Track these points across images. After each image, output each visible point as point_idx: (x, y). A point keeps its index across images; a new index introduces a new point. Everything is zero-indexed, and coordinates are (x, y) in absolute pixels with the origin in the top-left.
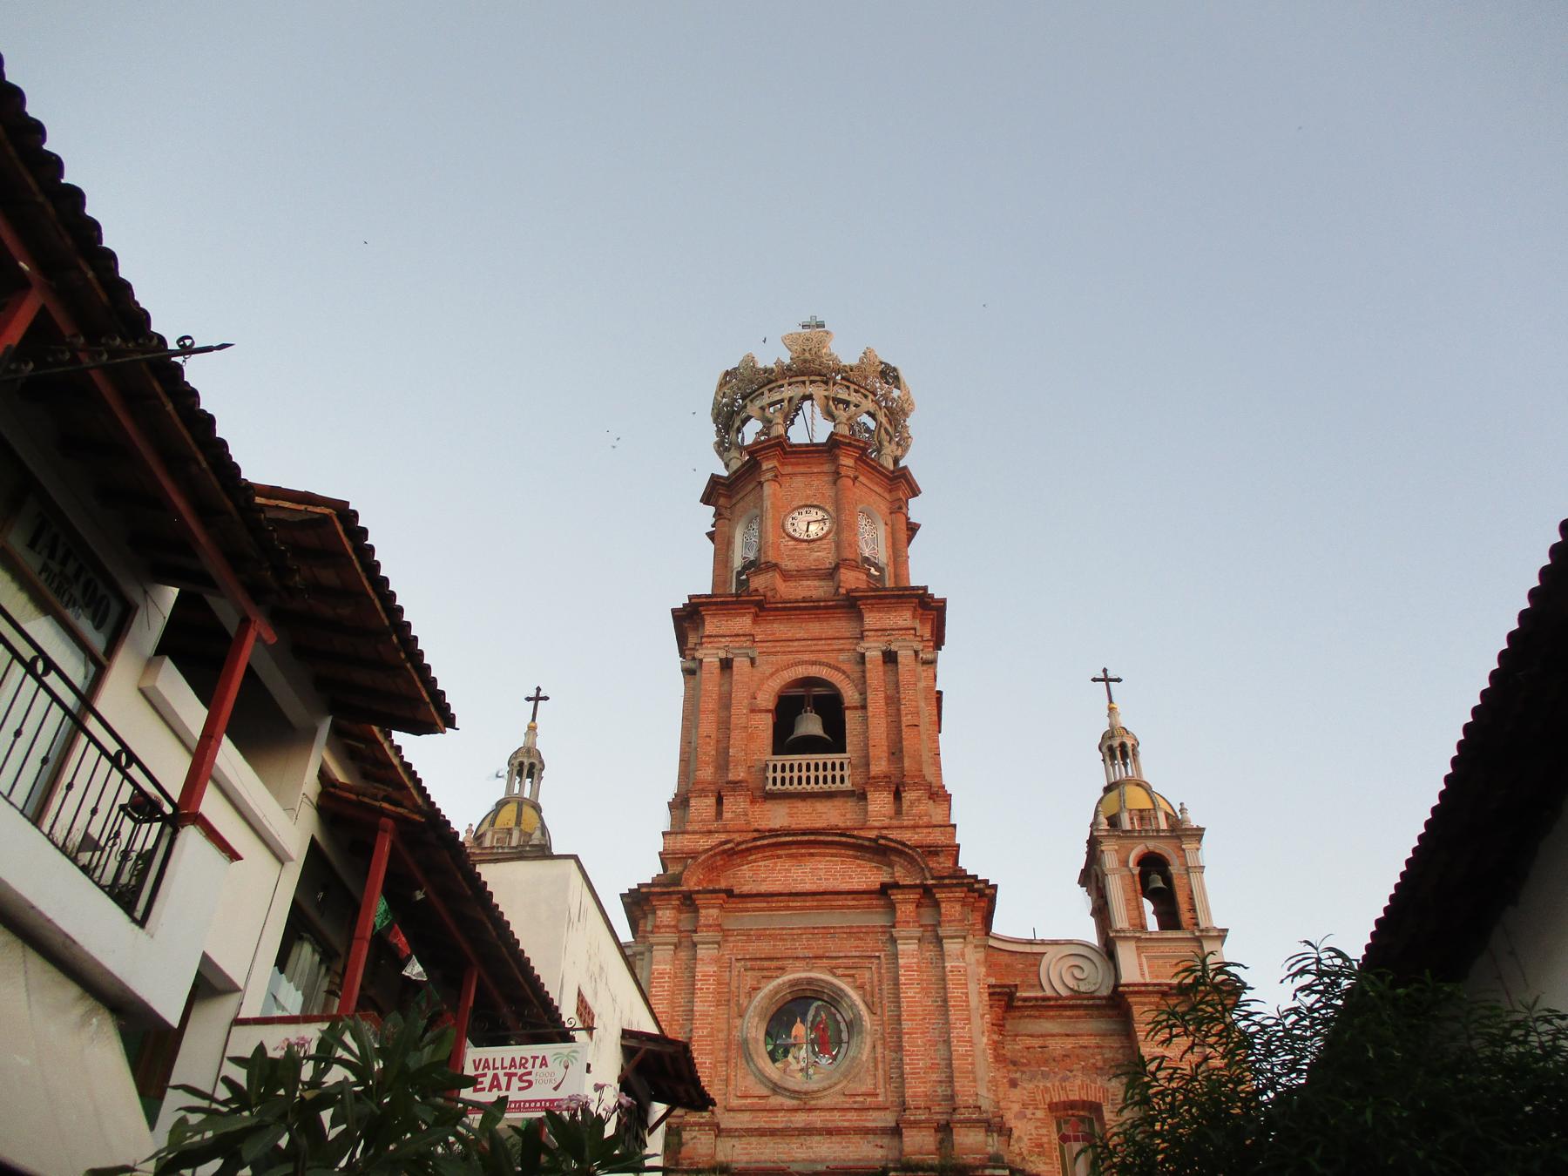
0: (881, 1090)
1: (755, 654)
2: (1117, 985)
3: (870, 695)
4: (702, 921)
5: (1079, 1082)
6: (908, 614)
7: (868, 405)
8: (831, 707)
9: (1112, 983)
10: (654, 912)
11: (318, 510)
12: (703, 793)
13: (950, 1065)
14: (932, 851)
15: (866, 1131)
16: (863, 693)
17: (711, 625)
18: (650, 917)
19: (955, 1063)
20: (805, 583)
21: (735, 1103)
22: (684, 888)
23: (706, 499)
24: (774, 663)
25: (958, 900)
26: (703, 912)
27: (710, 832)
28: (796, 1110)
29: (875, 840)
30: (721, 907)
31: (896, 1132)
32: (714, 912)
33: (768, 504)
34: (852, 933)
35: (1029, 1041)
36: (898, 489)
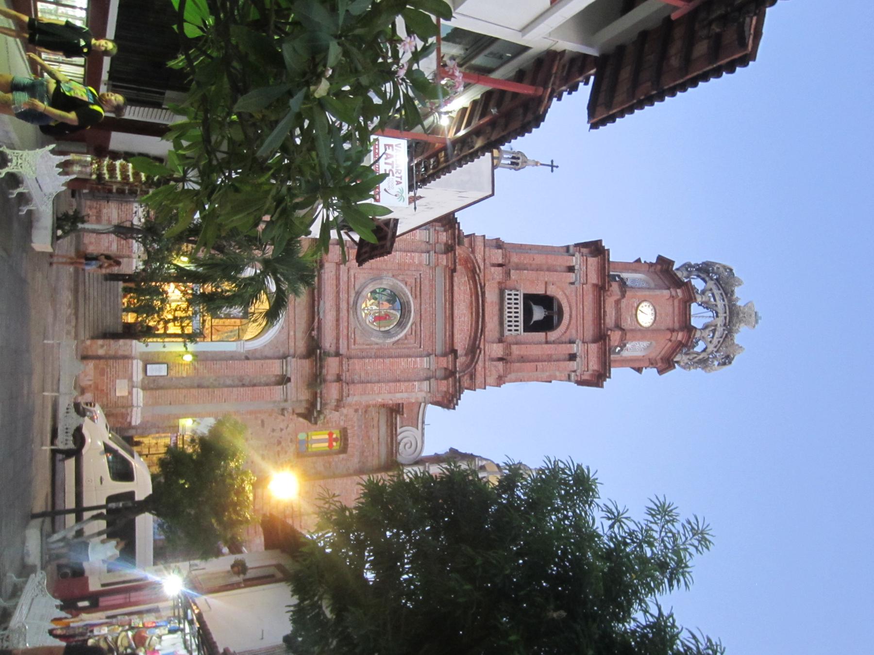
0: (357, 347)
1: (577, 284)
2: (402, 465)
3: (552, 346)
4: (440, 256)
5: (357, 443)
6: (596, 367)
7: (711, 348)
8: (546, 325)
9: (403, 462)
10: (446, 231)
11: (751, 42)
12: (504, 256)
13: (368, 382)
14: (472, 377)
15: (338, 339)
16: (554, 342)
17: (593, 261)
18: (442, 229)
19: (369, 385)
22: (457, 247)
23: (660, 259)
24: (572, 294)
25: (448, 389)
26: (445, 256)
27: (484, 260)
28: (348, 304)
29: (479, 347)
30: (447, 266)
31: (337, 354)
32: (445, 263)
33: (658, 292)
34: (432, 335)
35: (376, 420)
36: (662, 362)
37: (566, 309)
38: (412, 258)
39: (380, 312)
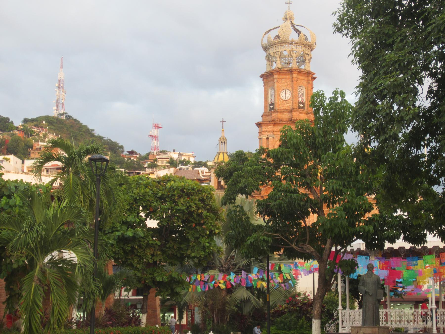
20: (285, 114)
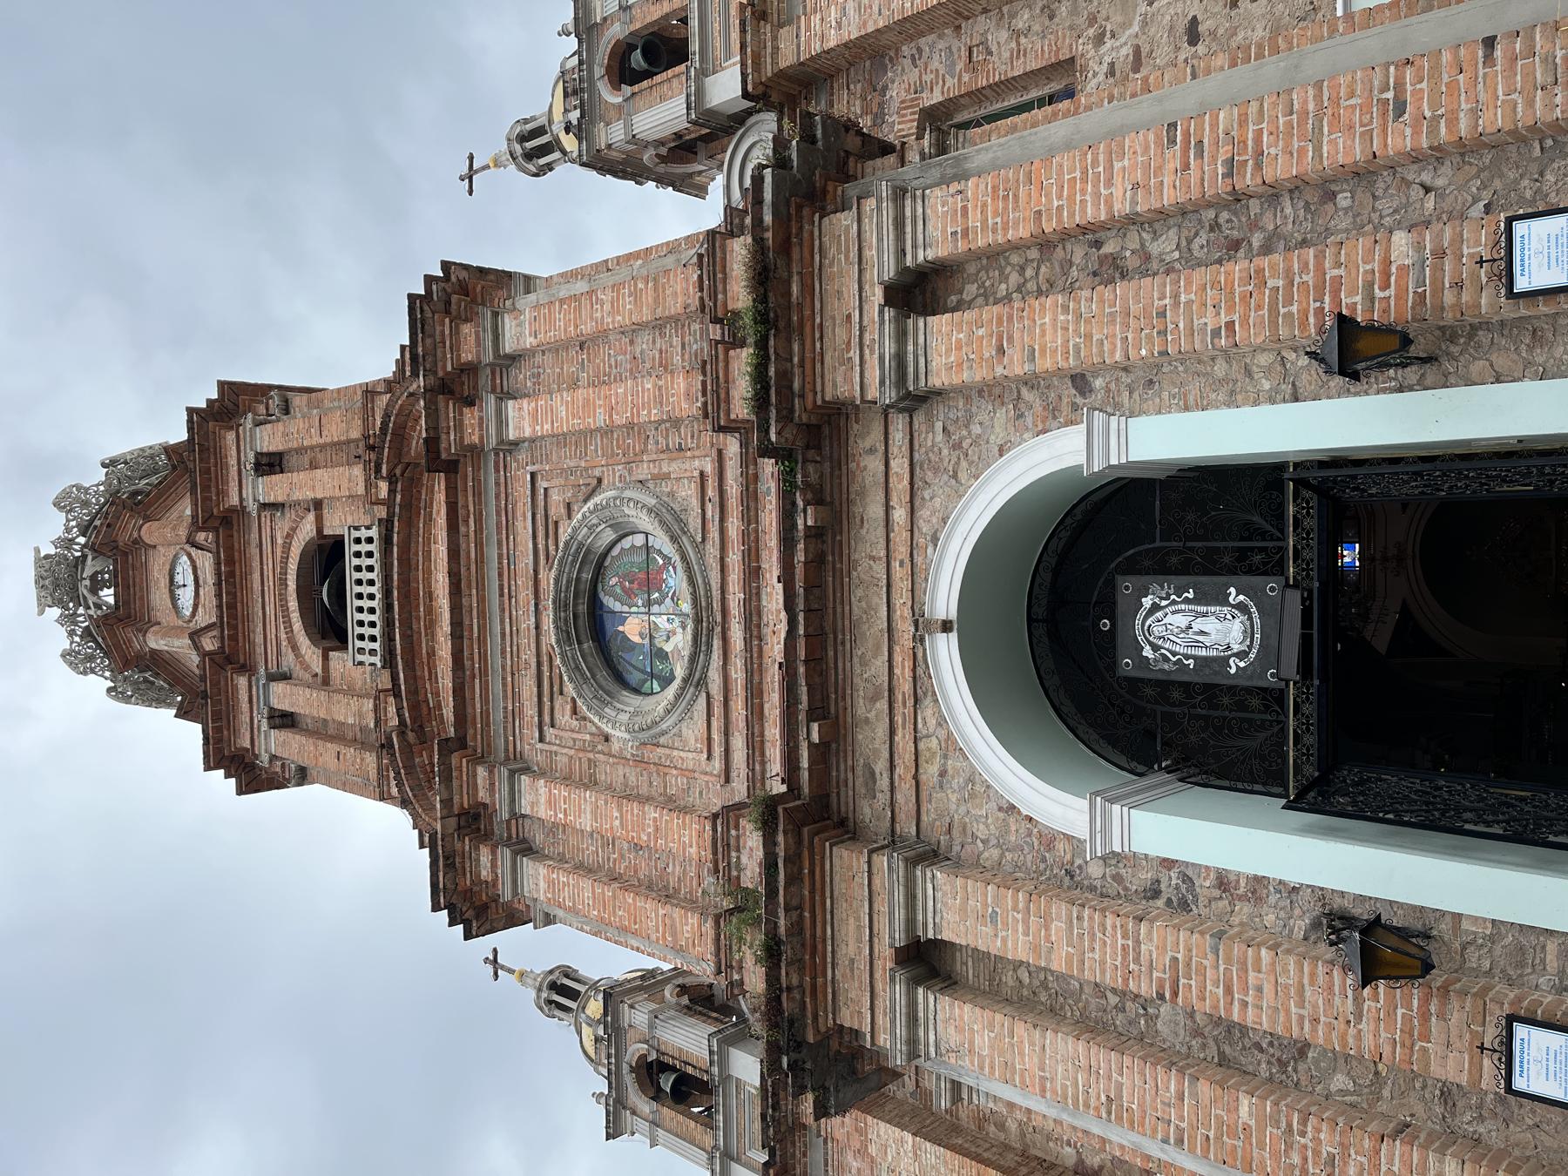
19: (646, 315)
21: (717, 764)
25: (455, 332)
37: (293, 604)
38: (551, 803)
39: (649, 603)
